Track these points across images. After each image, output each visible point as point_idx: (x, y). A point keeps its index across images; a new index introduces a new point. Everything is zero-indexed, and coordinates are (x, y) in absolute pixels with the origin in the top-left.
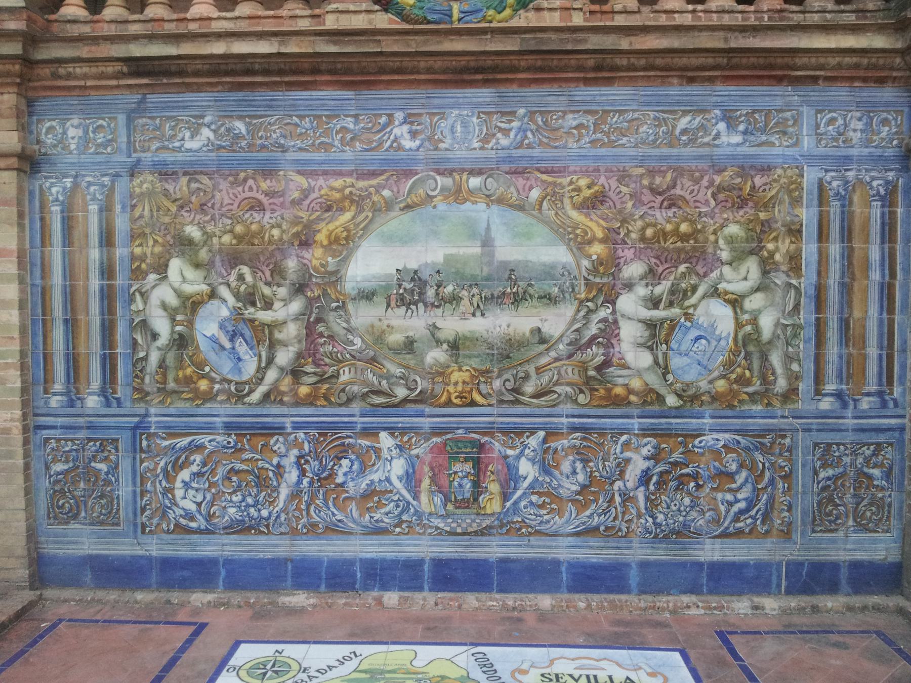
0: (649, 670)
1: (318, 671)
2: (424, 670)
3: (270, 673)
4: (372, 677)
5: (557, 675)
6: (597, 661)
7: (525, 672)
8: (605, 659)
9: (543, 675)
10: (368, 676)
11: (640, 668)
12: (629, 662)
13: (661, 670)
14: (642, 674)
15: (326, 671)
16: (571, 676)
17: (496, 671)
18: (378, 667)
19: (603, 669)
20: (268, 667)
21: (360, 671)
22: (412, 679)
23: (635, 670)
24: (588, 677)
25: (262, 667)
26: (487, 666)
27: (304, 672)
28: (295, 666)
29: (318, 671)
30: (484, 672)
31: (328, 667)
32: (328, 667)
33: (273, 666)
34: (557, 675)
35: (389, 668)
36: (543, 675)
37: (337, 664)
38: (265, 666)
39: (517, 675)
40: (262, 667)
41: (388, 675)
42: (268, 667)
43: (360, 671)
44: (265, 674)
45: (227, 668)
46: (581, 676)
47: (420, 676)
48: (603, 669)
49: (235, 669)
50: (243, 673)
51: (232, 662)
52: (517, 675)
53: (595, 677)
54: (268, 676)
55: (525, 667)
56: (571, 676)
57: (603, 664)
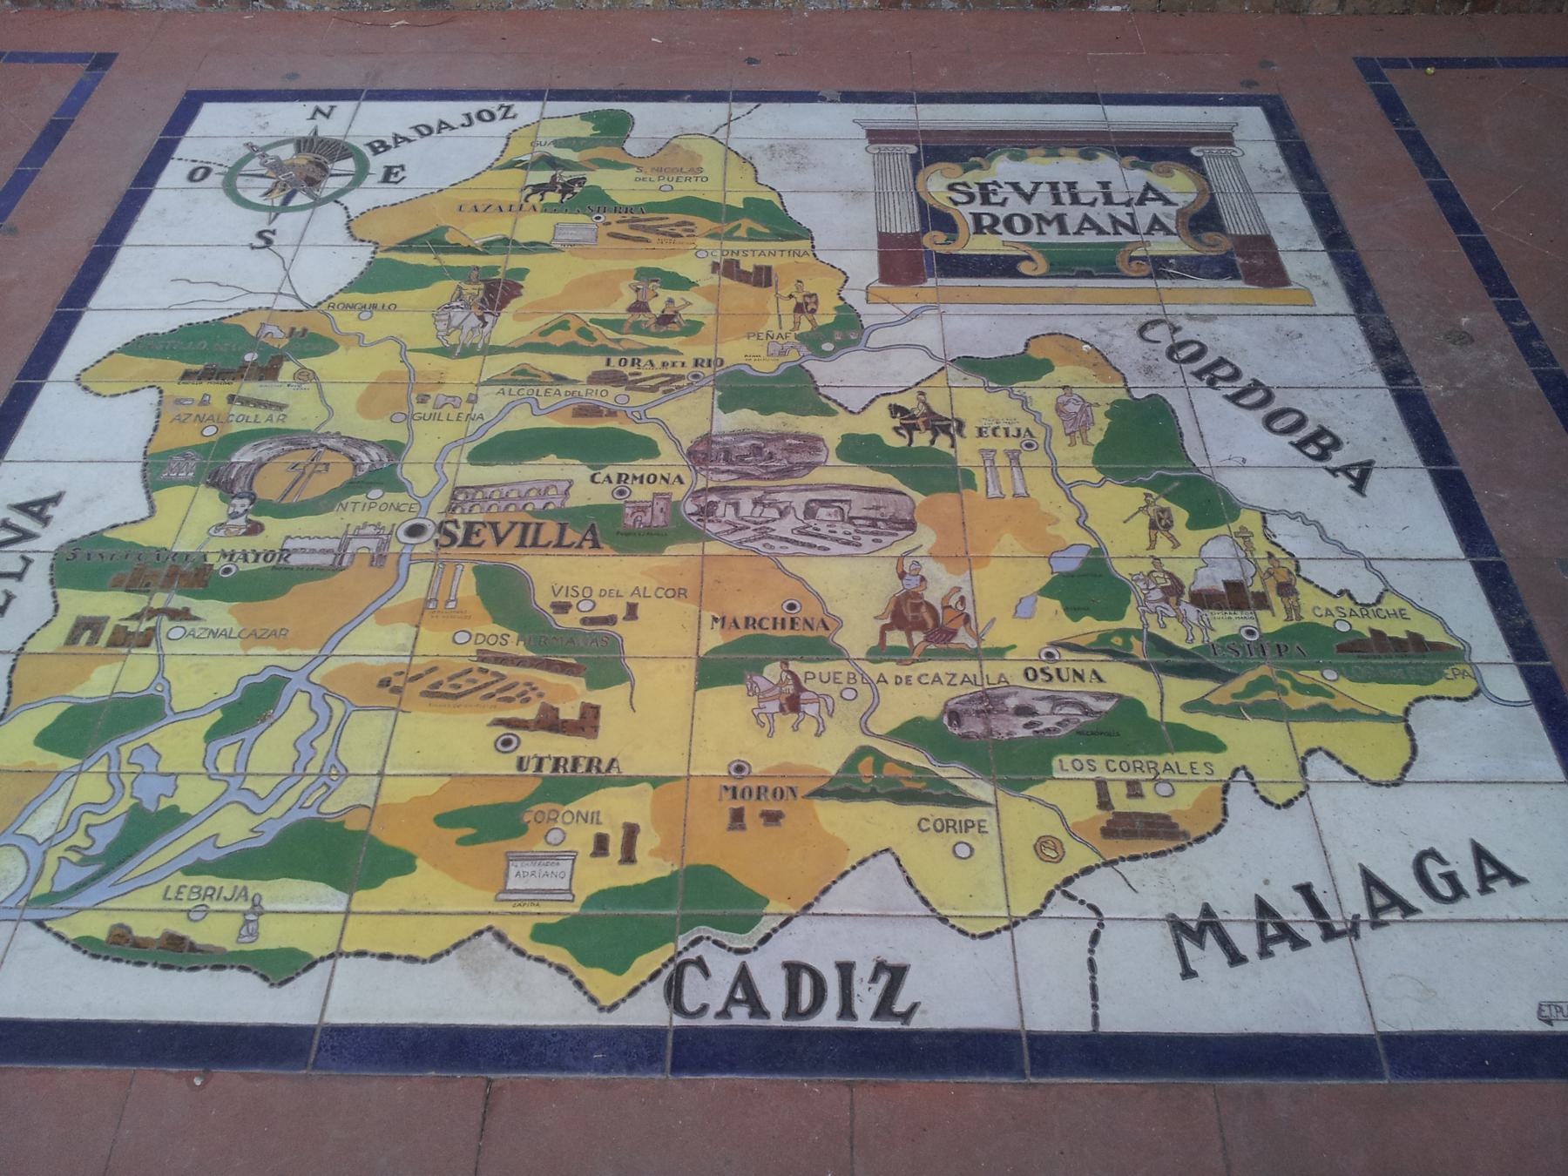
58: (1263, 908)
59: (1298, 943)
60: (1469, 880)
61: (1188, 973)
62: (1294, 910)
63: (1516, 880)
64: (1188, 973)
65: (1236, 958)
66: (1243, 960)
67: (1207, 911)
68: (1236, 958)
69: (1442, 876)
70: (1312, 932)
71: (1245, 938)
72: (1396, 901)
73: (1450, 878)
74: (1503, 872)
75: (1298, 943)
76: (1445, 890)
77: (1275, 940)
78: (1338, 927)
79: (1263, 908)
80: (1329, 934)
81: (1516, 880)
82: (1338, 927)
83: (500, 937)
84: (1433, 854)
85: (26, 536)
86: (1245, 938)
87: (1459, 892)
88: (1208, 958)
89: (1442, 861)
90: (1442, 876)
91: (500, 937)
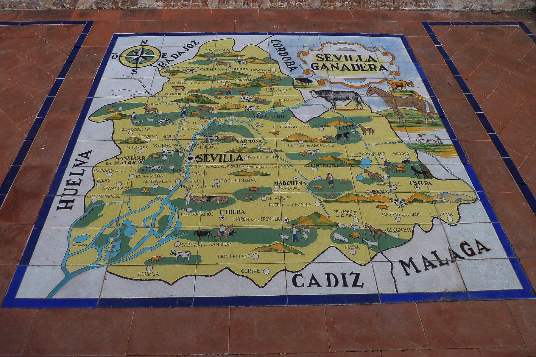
0: (383, 51)
1: (172, 56)
2: (241, 53)
3: (141, 59)
4: (208, 59)
5: (326, 55)
6: (351, 45)
7: (305, 54)
8: (355, 43)
9: (317, 56)
10: (206, 59)
11: (378, 50)
12: (371, 46)
13: (390, 51)
14: (378, 53)
15: (178, 56)
16: (335, 56)
17: (287, 53)
18: (211, 52)
19: (355, 51)
20: (139, 54)
21: (200, 56)
22: (234, 60)
23: (375, 51)
24: (345, 56)
25: (135, 54)
26: (282, 50)
27: (163, 57)
28: (157, 53)
29: (172, 56)
30: (280, 54)
31: (179, 52)
32: (179, 52)
33: (142, 53)
34: (326, 55)
35: (218, 53)
36: (317, 56)
37: (183, 50)
38: (137, 53)
39: (301, 56)
40: (135, 54)
41: (218, 58)
42: (139, 54)
43: (200, 56)
44: (138, 58)
45: (112, 55)
46: (341, 55)
47: (239, 58)
48: (355, 51)
49: (117, 56)
50: (123, 59)
51: (114, 51)
52: (301, 56)
53: (350, 56)
54: (139, 61)
55: (305, 50)
56: (335, 56)
57: (354, 47)
58: (424, 258)
59: (434, 266)
60: (476, 251)
61: (408, 274)
62: (432, 258)
63: (488, 250)
64: (408, 274)
65: (418, 271)
66: (420, 271)
67: (411, 259)
68: (418, 271)
69: (469, 249)
70: (437, 263)
71: (420, 265)
72: (457, 256)
73: (471, 249)
74: (484, 248)
75: (434, 266)
76: (469, 252)
77: (428, 266)
78: (444, 262)
79: (424, 258)
80: (442, 264)
81: (488, 250)
82: (444, 262)
83: (229, 270)
84: (466, 243)
85: (84, 163)
86: (420, 265)
87: (473, 254)
88: (411, 270)
89: (469, 246)
90: (469, 249)
91: (229, 270)
